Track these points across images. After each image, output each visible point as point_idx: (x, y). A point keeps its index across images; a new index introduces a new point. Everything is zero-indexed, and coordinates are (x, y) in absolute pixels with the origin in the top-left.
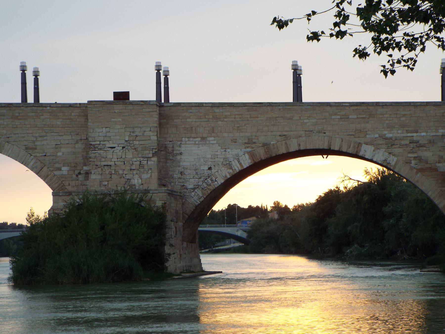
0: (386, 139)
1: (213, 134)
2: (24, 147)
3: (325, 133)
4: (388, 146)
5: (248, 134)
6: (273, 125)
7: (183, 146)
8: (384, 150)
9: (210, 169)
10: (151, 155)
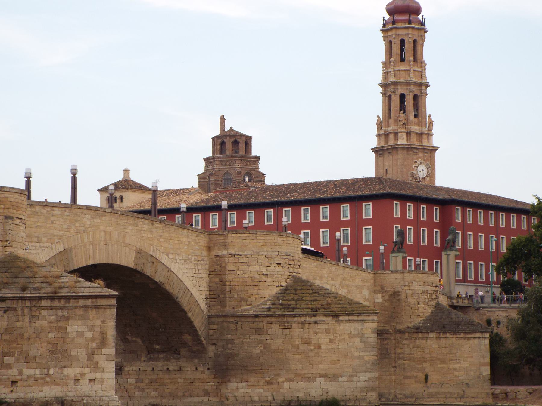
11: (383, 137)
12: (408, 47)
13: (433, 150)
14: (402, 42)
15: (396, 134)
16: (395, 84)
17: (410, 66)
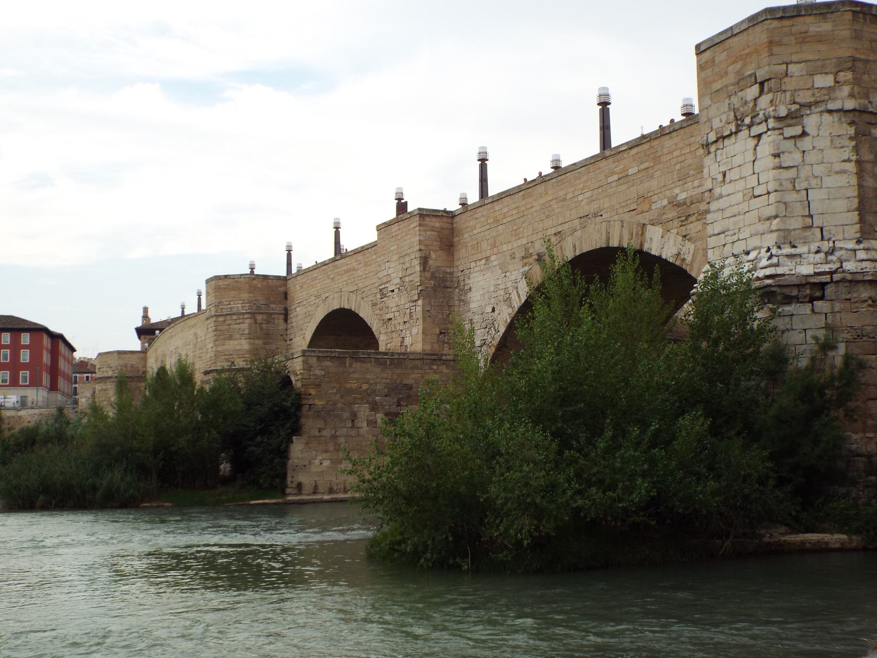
0: (678, 205)
1: (495, 250)
3: (601, 215)
4: (682, 221)
5: (524, 241)
7: (471, 276)
8: (676, 230)
9: (493, 310)
10: (416, 297)
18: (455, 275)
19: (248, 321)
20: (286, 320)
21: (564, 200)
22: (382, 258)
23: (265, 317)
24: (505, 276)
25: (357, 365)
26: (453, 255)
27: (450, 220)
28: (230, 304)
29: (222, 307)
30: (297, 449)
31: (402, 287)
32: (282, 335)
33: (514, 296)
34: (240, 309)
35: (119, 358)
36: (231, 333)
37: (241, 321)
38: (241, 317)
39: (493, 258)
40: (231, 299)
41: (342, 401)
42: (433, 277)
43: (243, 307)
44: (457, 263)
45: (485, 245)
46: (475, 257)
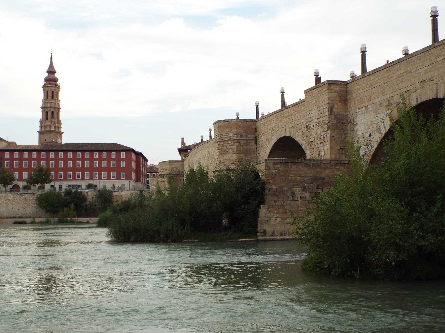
1: (371, 102)
2: (301, 133)
3: (433, 80)
5: (388, 96)
6: (401, 82)
7: (357, 117)
9: (370, 135)
10: (326, 129)
11: (43, 127)
12: (55, 94)
13: (62, 133)
14: (53, 92)
15: (50, 126)
16: (50, 107)
17: (56, 101)
18: (348, 116)
19: (236, 144)
20: (256, 143)
21: (411, 72)
22: (308, 108)
23: (245, 142)
24: (377, 116)
25: (294, 167)
26: (347, 105)
27: (345, 86)
28: (226, 135)
29: (222, 137)
30: (263, 212)
31: (319, 123)
32: (254, 151)
33: (382, 127)
34: (232, 138)
35: (170, 164)
36: (228, 151)
37: (232, 144)
38: (232, 142)
39: (370, 106)
40: (227, 133)
41: (287, 186)
42: (336, 117)
43: (233, 136)
44: (349, 110)
45: (365, 99)
46: (359, 106)
